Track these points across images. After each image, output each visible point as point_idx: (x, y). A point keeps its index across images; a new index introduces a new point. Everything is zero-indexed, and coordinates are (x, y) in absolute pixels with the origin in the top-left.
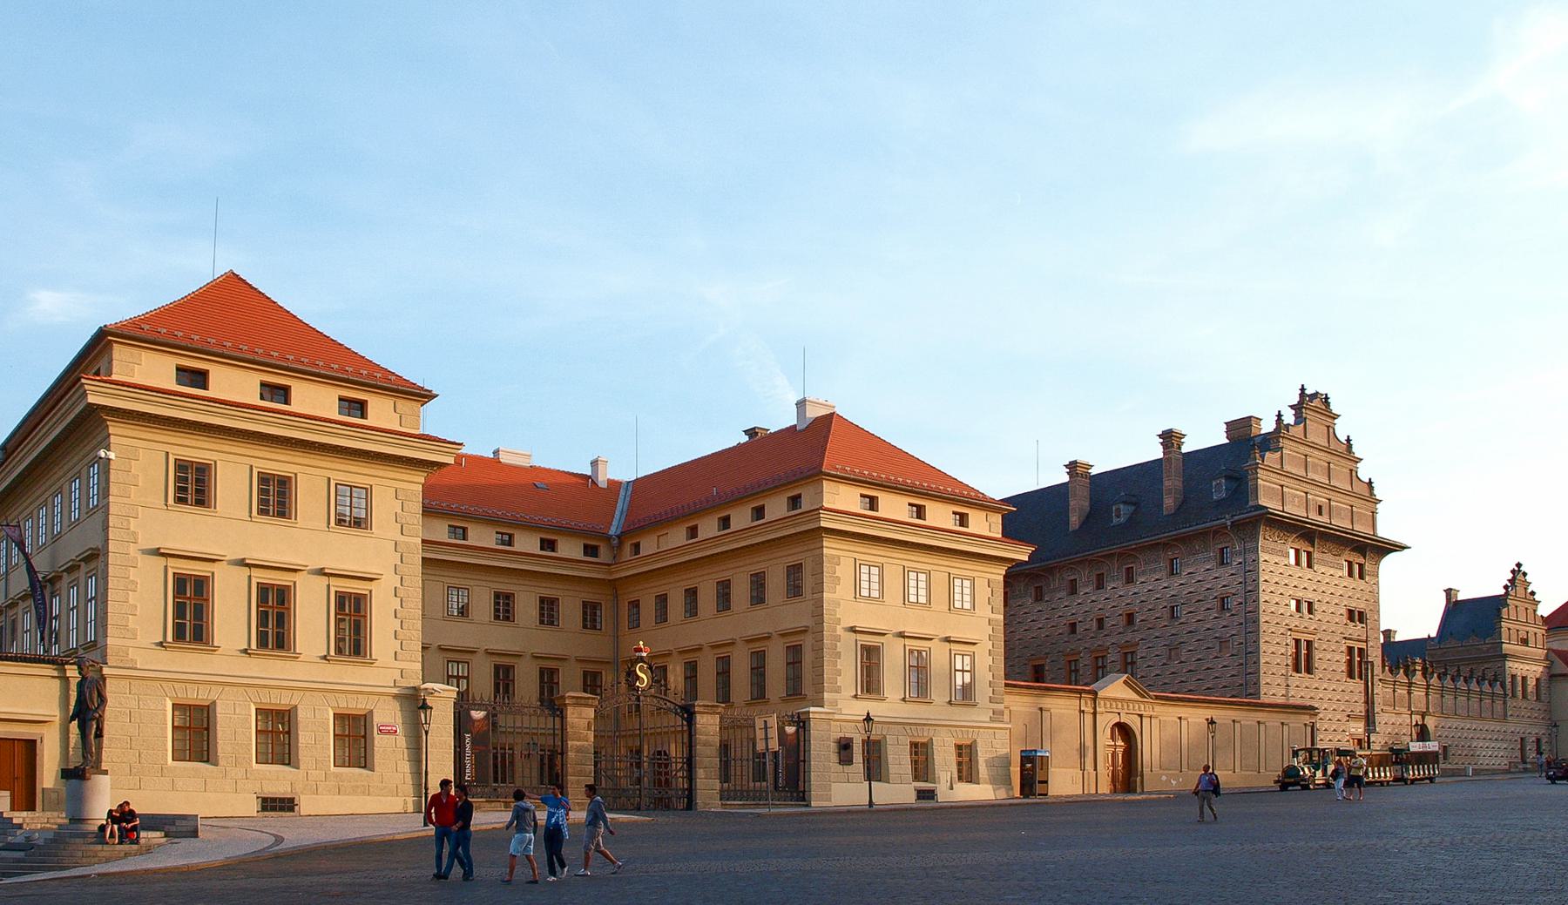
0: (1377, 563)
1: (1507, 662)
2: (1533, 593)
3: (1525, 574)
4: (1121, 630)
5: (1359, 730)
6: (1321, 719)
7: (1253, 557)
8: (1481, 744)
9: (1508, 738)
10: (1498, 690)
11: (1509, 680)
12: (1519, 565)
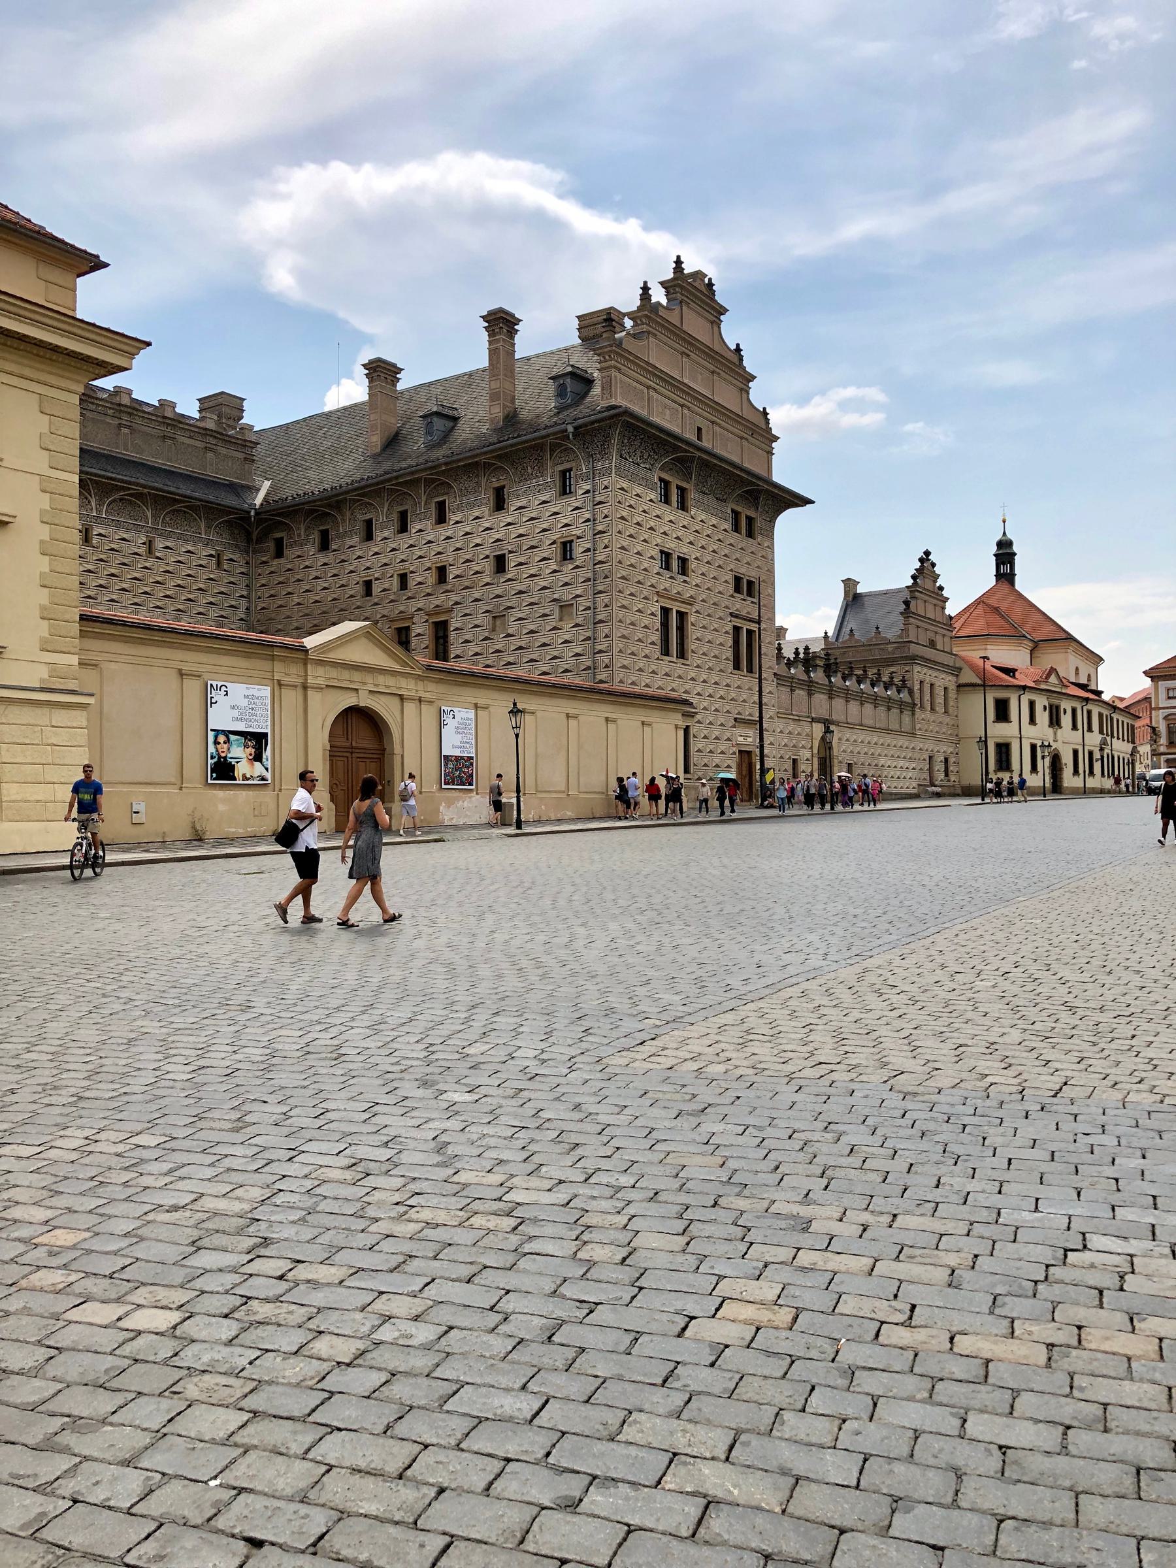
0: (772, 520)
1: (915, 666)
2: (941, 588)
3: (933, 565)
4: (429, 591)
5: (749, 739)
6: (699, 722)
7: (606, 483)
8: (889, 763)
9: (917, 755)
10: (904, 695)
11: (917, 687)
12: (927, 553)
